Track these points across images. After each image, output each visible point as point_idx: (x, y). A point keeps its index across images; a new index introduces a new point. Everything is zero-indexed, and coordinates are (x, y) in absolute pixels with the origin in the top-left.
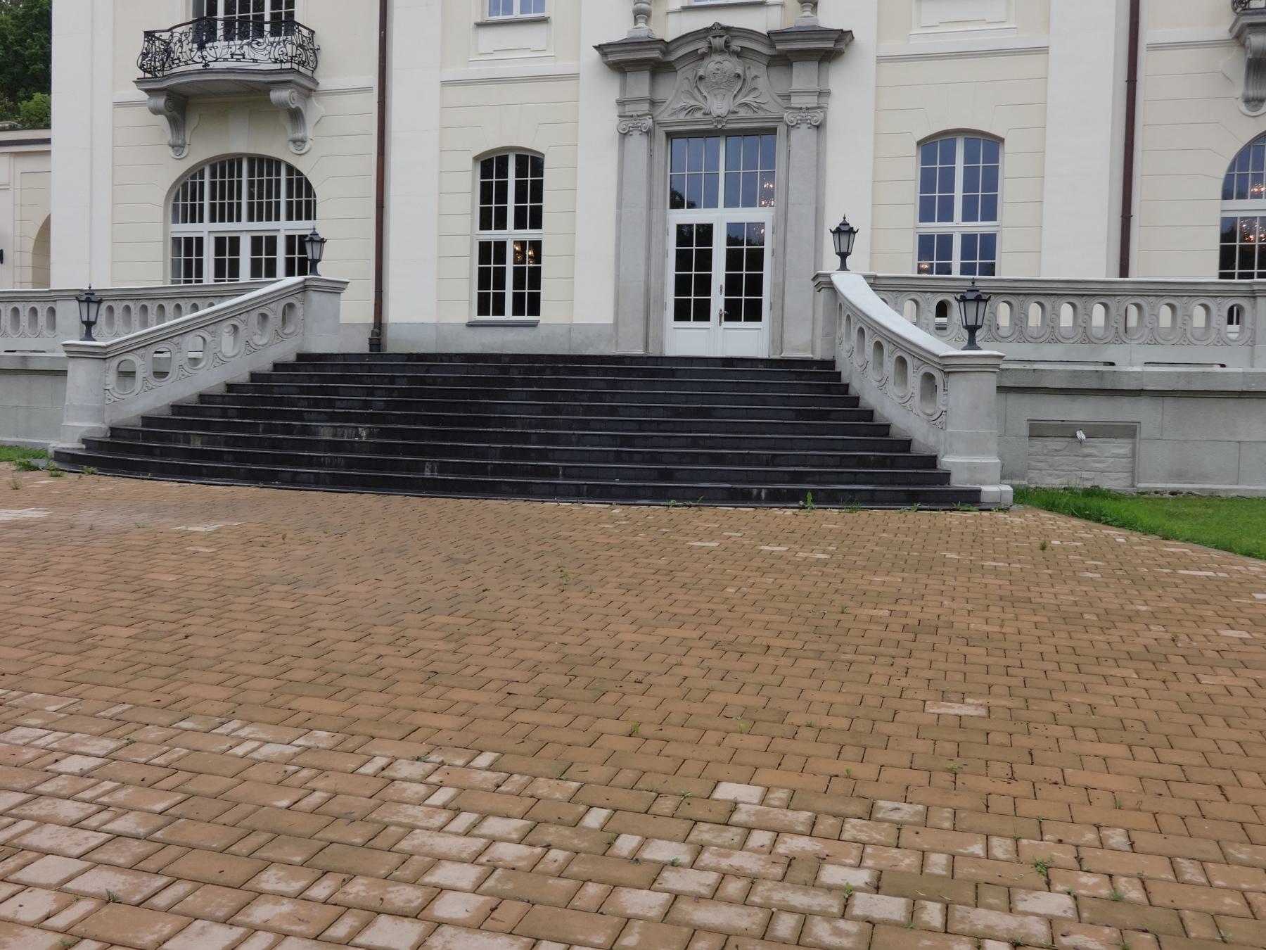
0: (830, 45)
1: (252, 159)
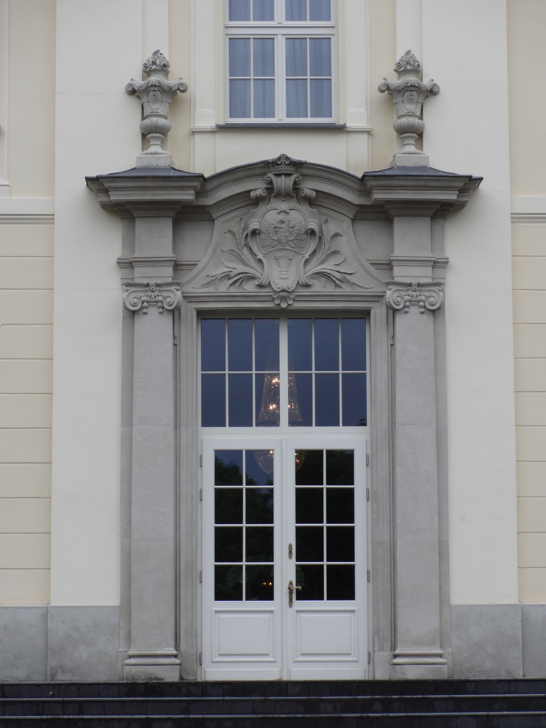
0: (452, 196)
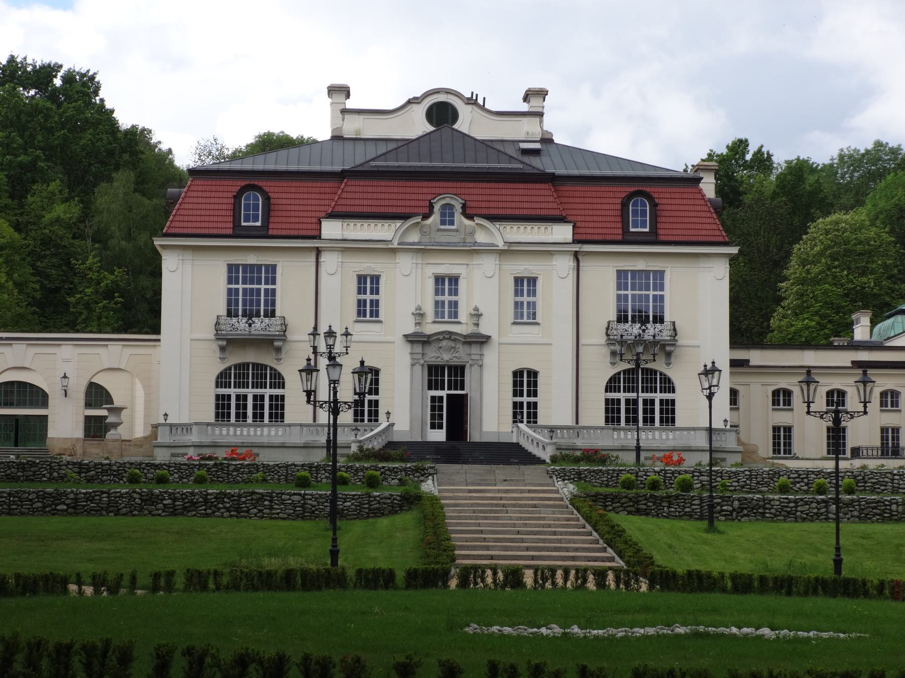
1: (253, 364)
